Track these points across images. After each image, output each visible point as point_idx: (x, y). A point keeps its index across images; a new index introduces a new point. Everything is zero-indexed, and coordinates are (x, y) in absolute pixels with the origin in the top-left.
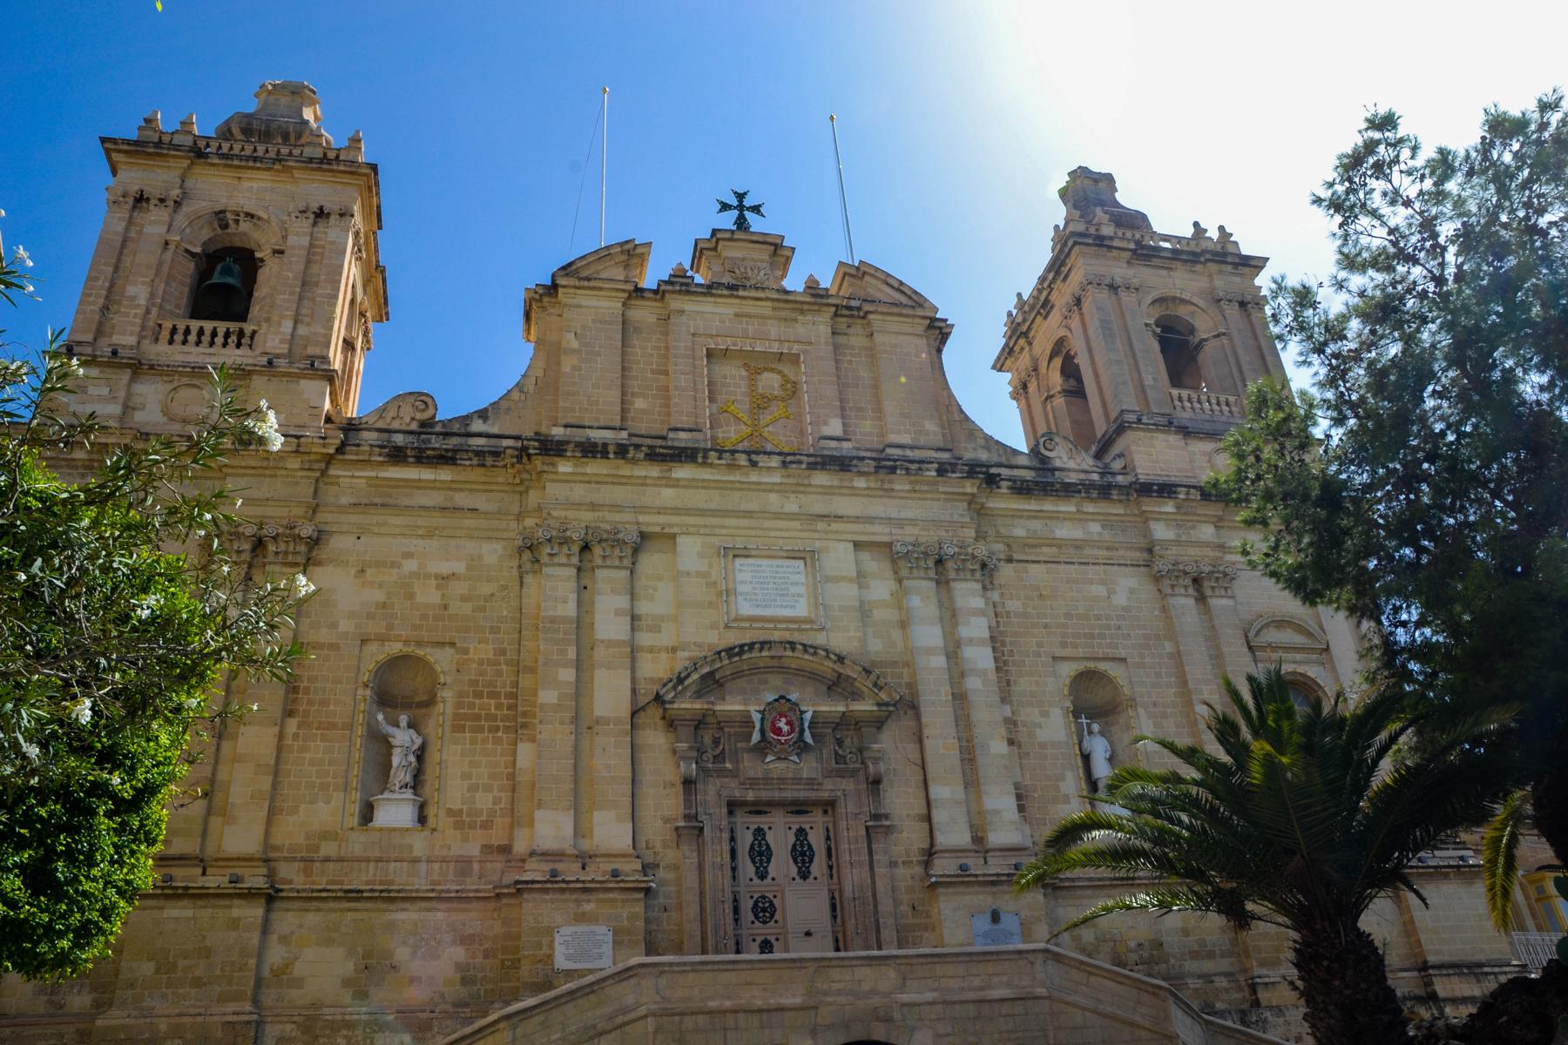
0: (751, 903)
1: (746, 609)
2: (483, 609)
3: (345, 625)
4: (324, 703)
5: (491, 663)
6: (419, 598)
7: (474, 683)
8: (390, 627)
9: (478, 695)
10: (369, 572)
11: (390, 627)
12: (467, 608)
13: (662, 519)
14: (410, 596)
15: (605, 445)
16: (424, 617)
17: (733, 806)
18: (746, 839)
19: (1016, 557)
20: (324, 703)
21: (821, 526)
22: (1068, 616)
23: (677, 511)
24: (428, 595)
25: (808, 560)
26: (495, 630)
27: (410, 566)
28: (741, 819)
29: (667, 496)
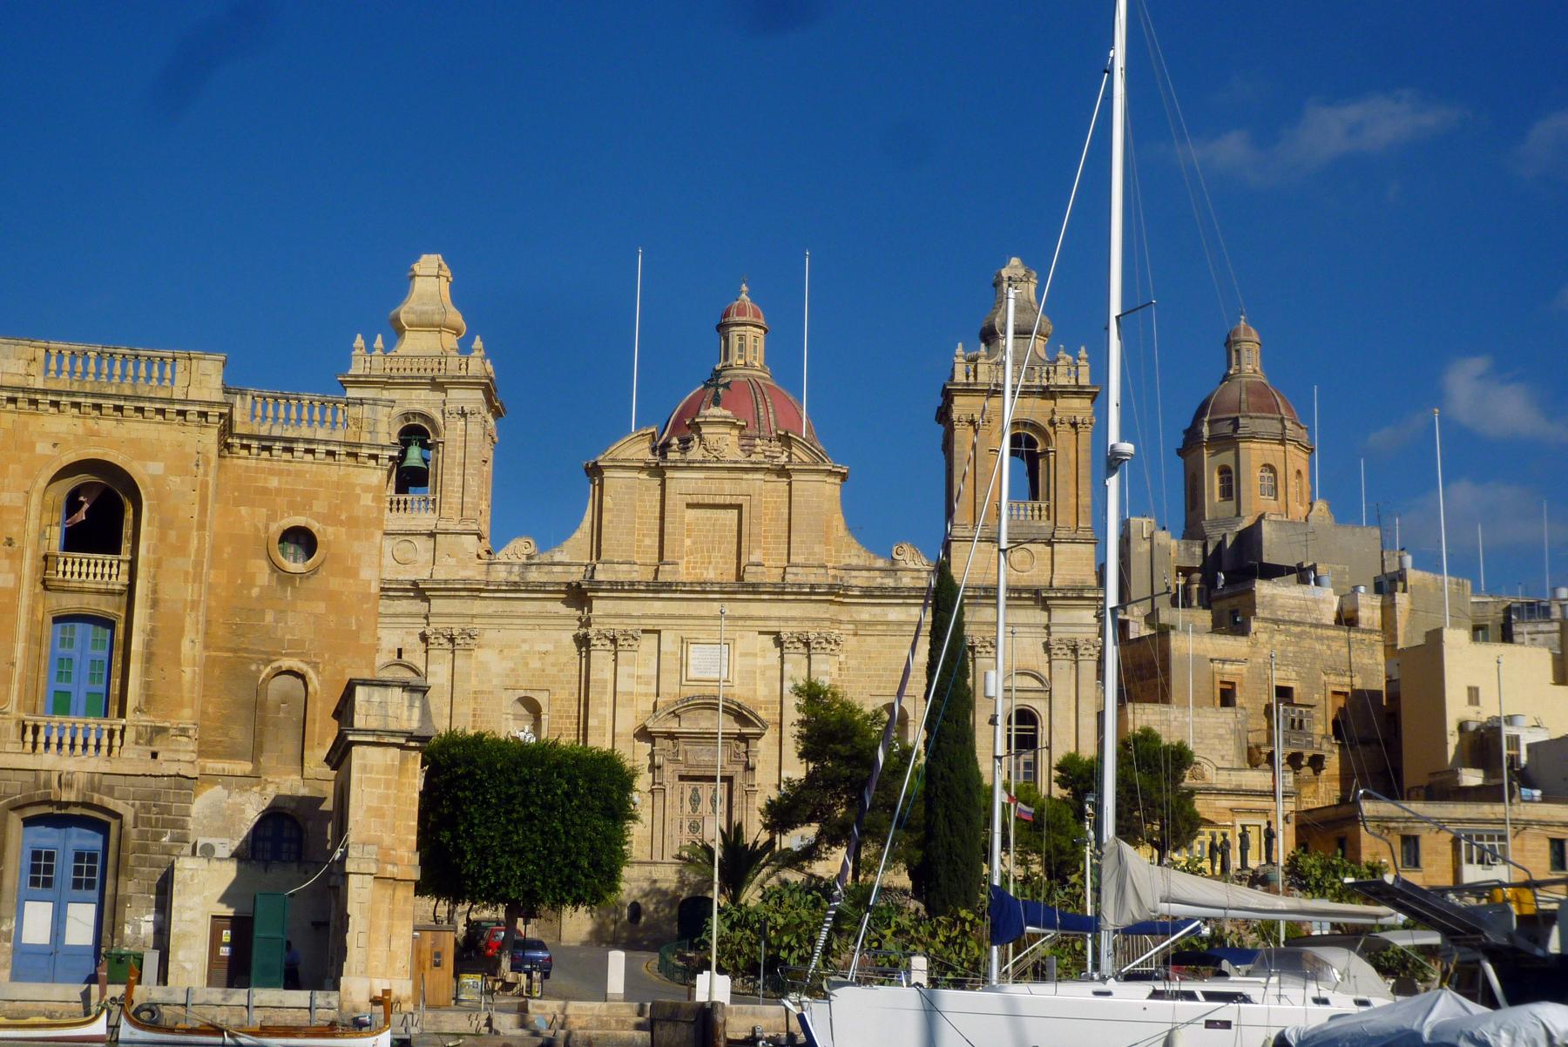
0: (688, 824)
1: (693, 674)
2: (562, 670)
3: (495, 681)
4: (488, 722)
5: (567, 700)
6: (531, 666)
7: (559, 711)
8: (517, 681)
9: (561, 717)
10: (506, 651)
11: (517, 681)
12: (554, 671)
13: (653, 621)
14: (526, 664)
15: (622, 582)
16: (533, 675)
17: (682, 778)
18: (688, 793)
19: (860, 632)
20: (488, 722)
21: (740, 623)
22: (885, 669)
23: (661, 617)
24: (535, 664)
25: (731, 646)
26: (569, 682)
27: (525, 647)
28: (688, 787)
29: (657, 607)
